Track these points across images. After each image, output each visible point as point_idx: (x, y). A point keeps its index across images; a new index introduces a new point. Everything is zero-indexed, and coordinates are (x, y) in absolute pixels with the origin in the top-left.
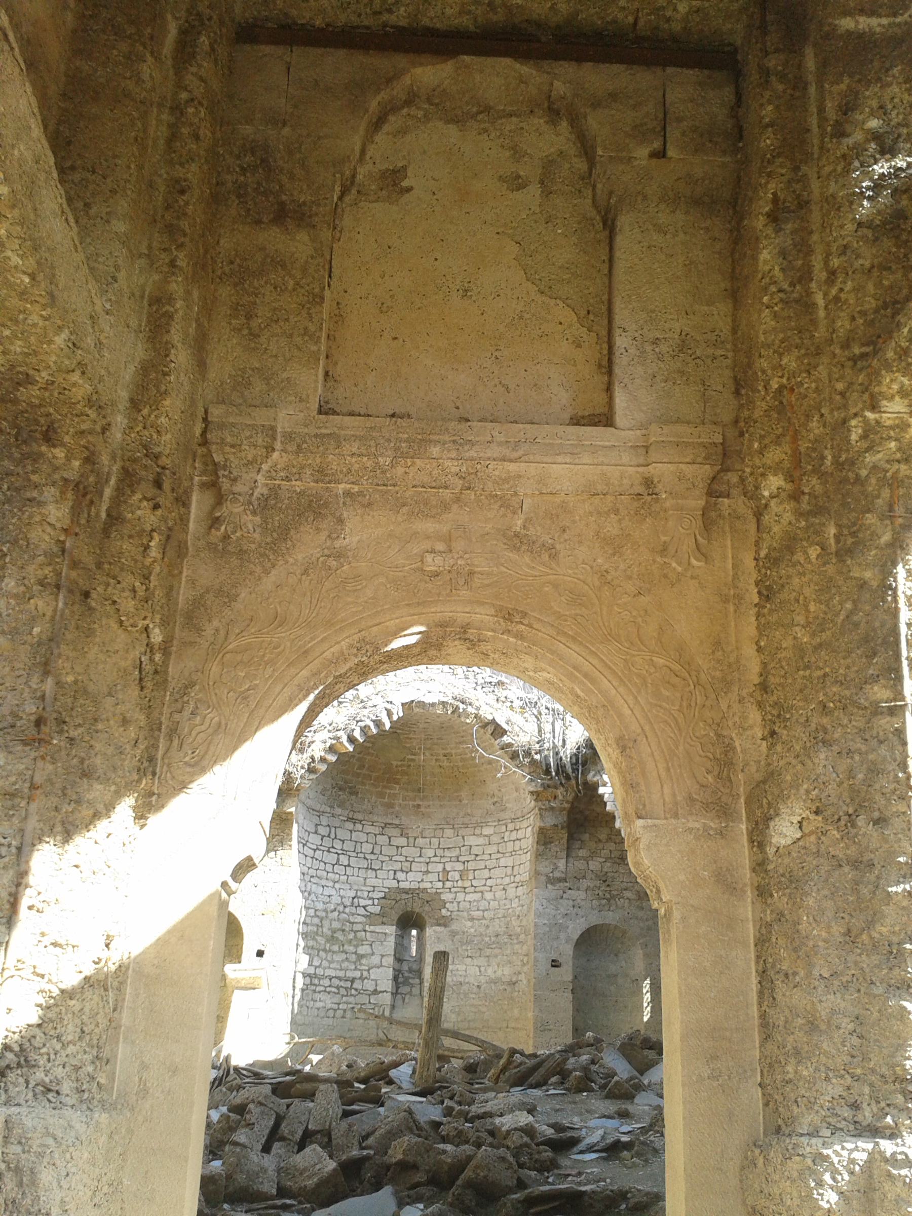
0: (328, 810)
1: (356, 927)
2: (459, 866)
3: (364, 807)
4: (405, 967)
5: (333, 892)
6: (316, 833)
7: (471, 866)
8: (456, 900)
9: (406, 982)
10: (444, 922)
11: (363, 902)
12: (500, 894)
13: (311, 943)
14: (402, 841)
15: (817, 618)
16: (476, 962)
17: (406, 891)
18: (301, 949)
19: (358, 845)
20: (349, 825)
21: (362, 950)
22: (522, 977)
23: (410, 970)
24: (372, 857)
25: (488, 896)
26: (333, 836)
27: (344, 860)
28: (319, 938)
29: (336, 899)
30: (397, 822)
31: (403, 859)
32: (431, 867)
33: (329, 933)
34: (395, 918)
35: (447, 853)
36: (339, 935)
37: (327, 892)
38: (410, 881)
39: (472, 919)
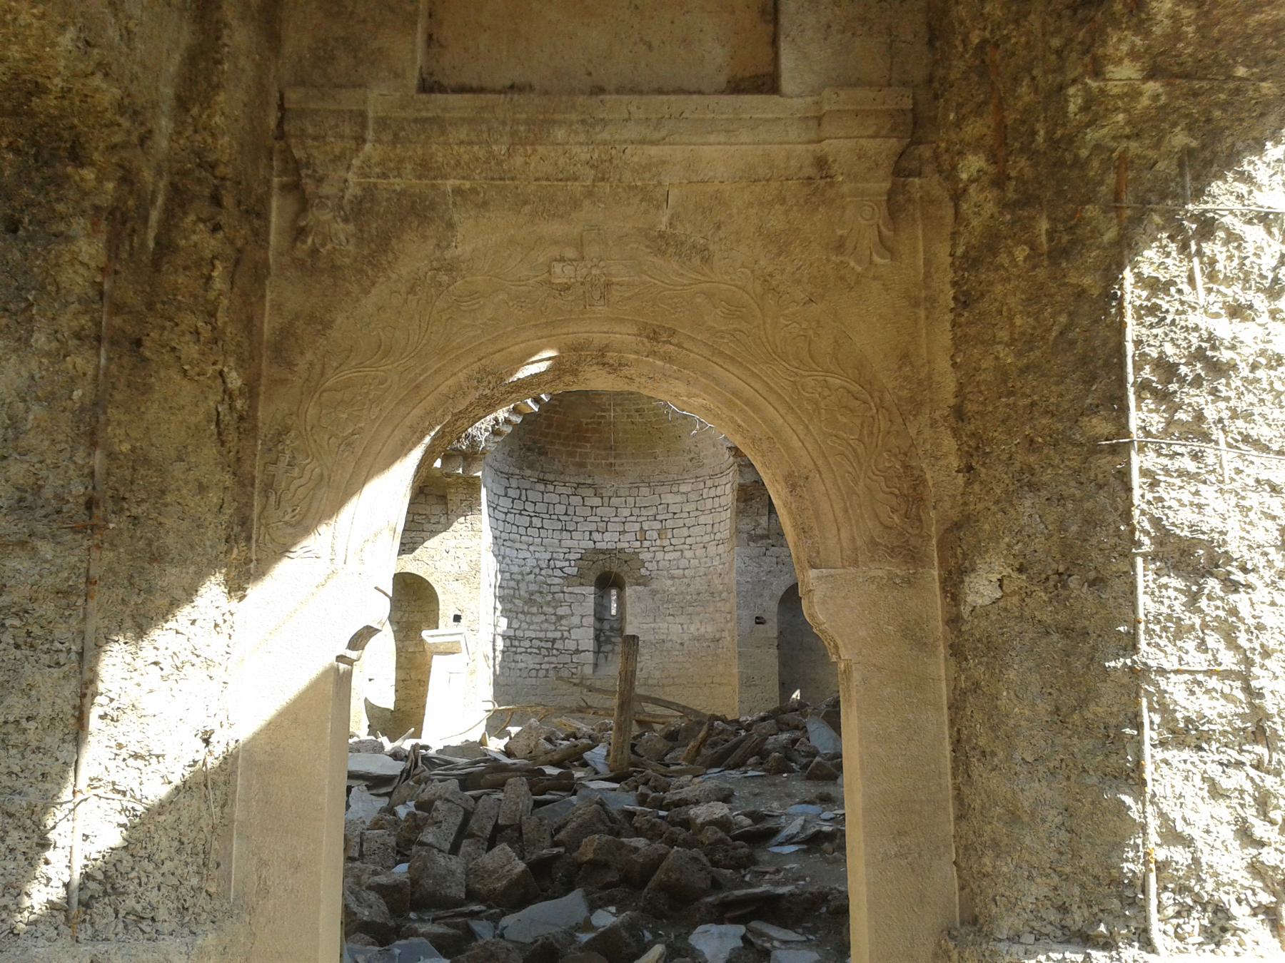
0: (517, 471)
1: (554, 589)
2: (657, 525)
4: (606, 626)
7: (669, 524)
8: (655, 559)
9: (608, 641)
10: (643, 581)
11: (559, 564)
12: (700, 552)
13: (509, 606)
14: (597, 501)
15: (1023, 334)
16: (677, 620)
17: (603, 552)
18: (498, 613)
20: (541, 487)
21: (560, 611)
22: (726, 634)
23: (612, 629)
24: (566, 518)
25: (688, 554)
26: (524, 498)
28: (517, 601)
30: (589, 481)
31: (598, 519)
32: (627, 527)
33: (527, 595)
35: (644, 512)
36: (537, 597)
37: (522, 554)
38: (607, 541)
39: (673, 578)
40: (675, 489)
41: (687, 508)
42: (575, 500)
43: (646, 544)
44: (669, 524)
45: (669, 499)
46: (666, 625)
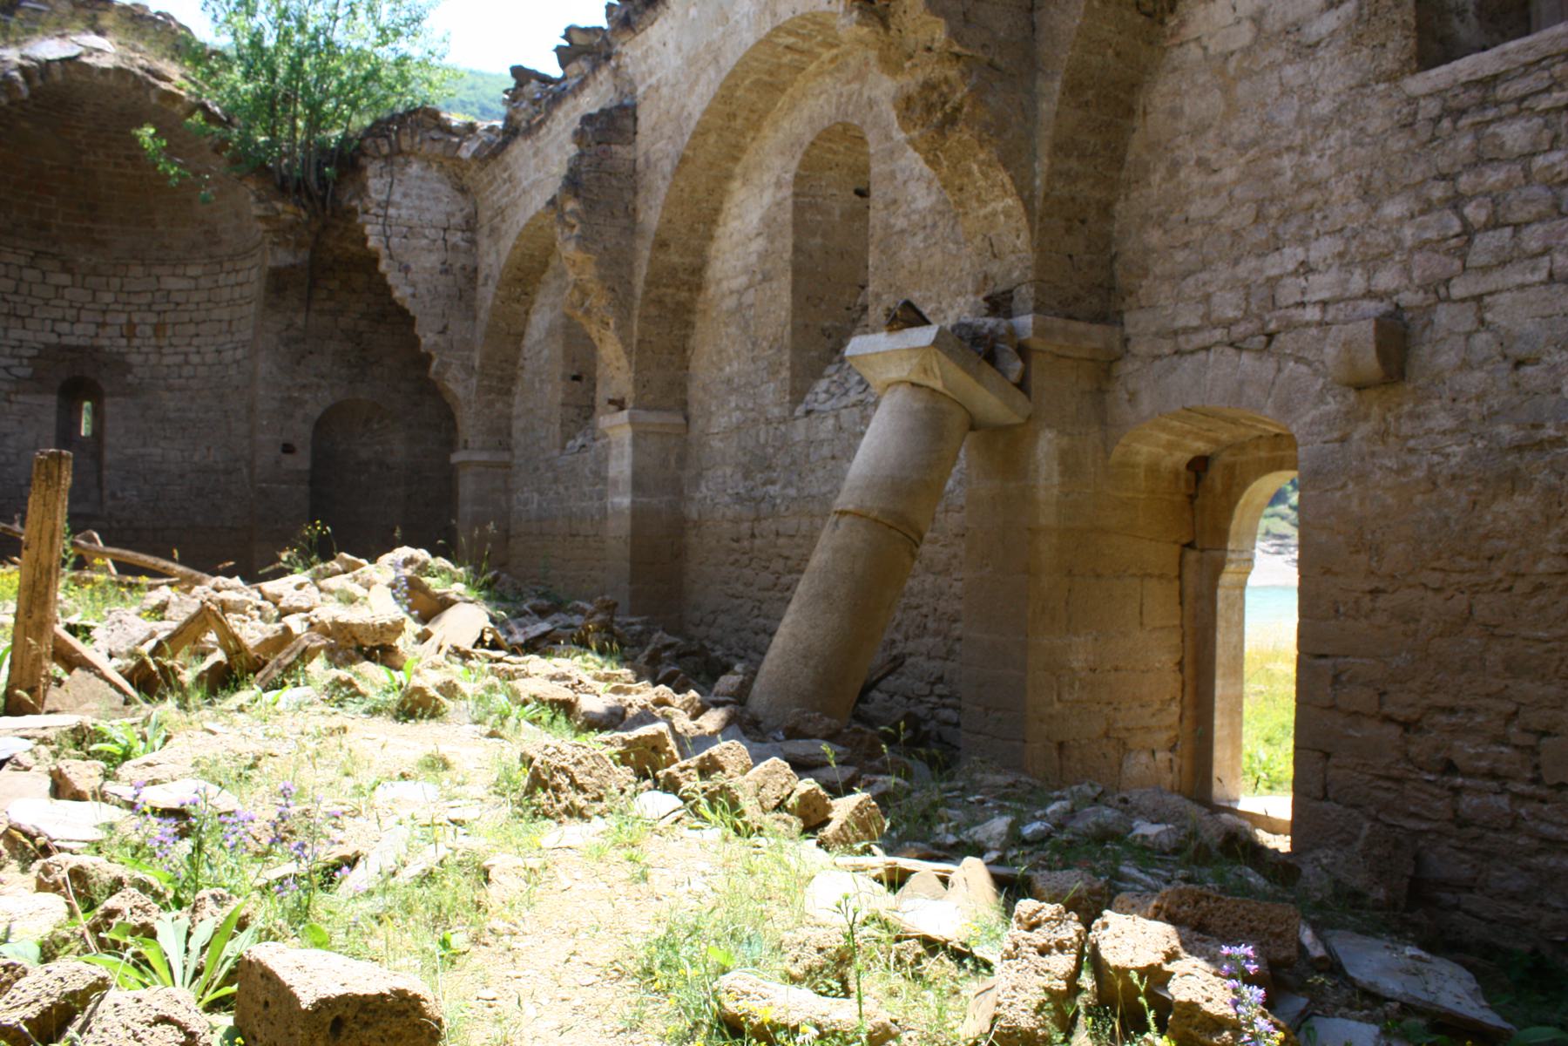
2: (153, 318)
14: (65, 279)
25: (195, 359)
30: (55, 250)
31: (66, 304)
32: (109, 318)
35: (134, 299)
38: (79, 334)
40: (180, 271)
41: (196, 297)
42: (30, 274)
43: (136, 342)
44: (170, 317)
45: (171, 283)
46: (159, 451)
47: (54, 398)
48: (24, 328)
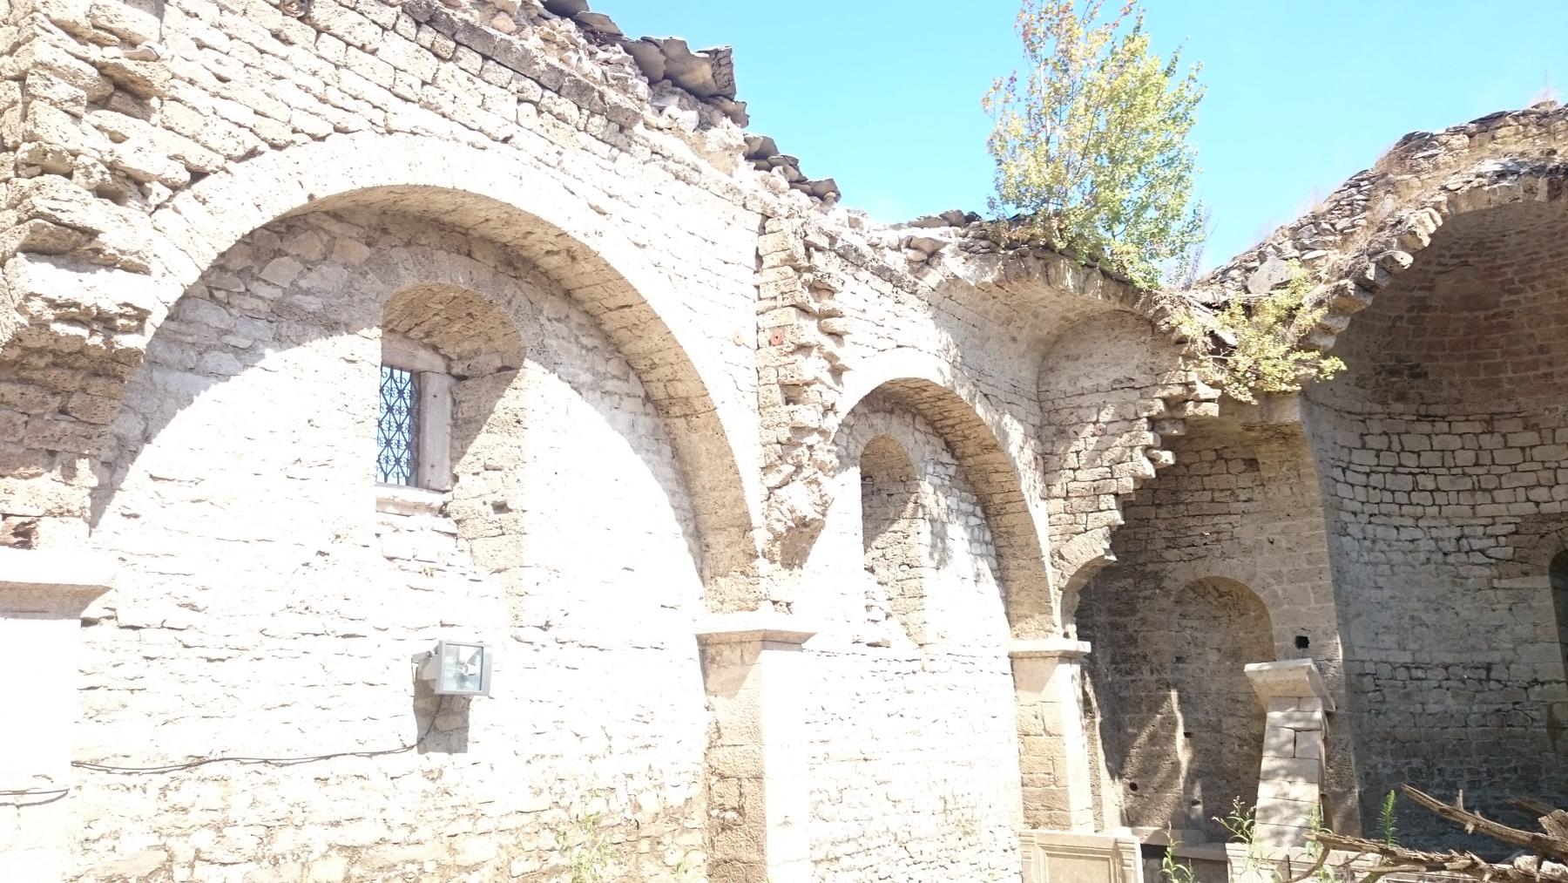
0: (1378, 408)
3: (1444, 394)
5: (1418, 534)
6: (1364, 447)
11: (1477, 544)
14: (1530, 438)
19: (1448, 455)
20: (1425, 427)
24: (1481, 471)
26: (1396, 447)
27: (1426, 482)
29: (1426, 545)
30: (1511, 408)
34: (1547, 563)
37: (1406, 534)
42: (1486, 440)
47: (1543, 583)
48: (1494, 502)
